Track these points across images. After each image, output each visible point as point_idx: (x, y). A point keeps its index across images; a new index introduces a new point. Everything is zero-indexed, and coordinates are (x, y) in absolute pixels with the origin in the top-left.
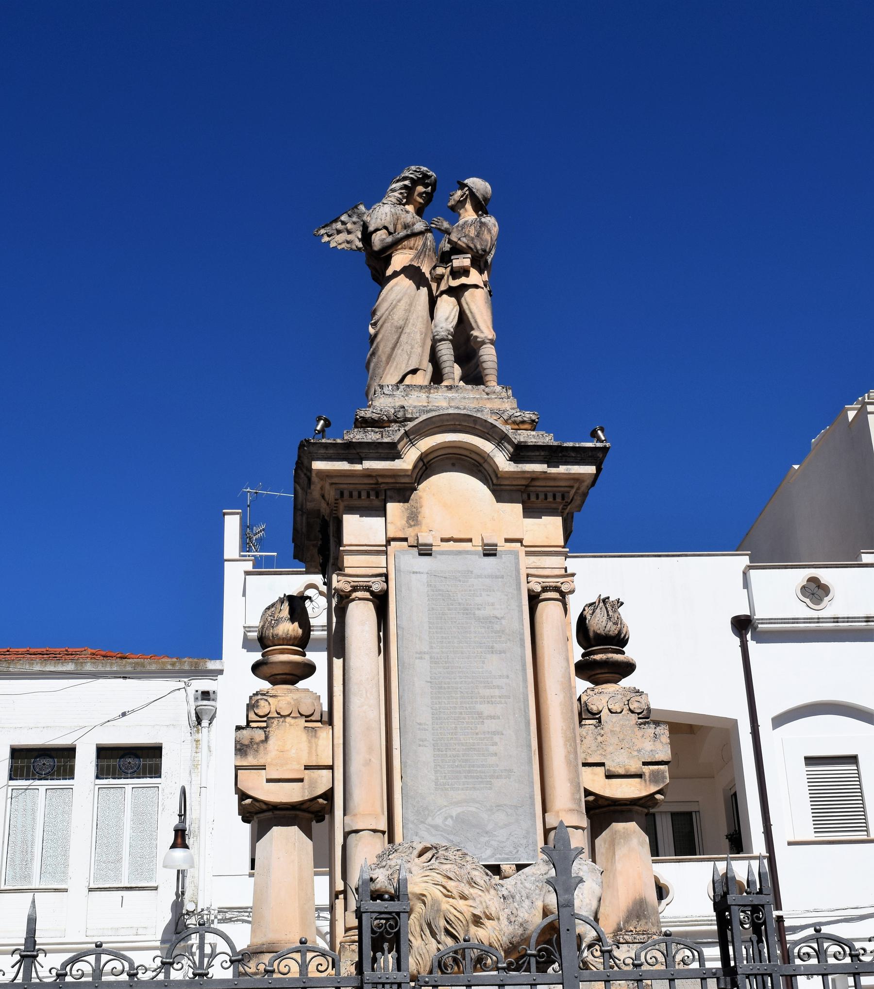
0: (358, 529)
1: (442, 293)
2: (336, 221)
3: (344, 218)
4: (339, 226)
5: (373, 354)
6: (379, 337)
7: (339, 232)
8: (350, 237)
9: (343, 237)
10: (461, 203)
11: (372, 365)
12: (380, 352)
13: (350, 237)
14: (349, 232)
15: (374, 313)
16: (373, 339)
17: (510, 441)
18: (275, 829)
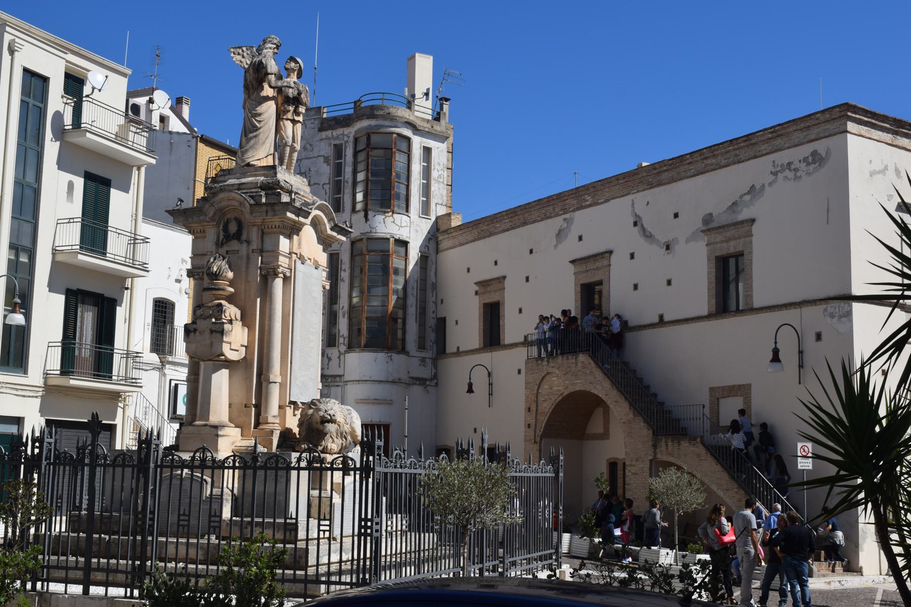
0: (284, 244)
1: (287, 119)
2: (240, 48)
3: (244, 49)
4: (240, 51)
5: (256, 136)
6: (261, 130)
7: (239, 54)
8: (243, 60)
9: (239, 57)
10: (293, 71)
11: (252, 142)
12: (261, 137)
13: (243, 60)
14: (243, 57)
15: (260, 115)
16: (257, 129)
17: (334, 221)
18: (224, 370)
